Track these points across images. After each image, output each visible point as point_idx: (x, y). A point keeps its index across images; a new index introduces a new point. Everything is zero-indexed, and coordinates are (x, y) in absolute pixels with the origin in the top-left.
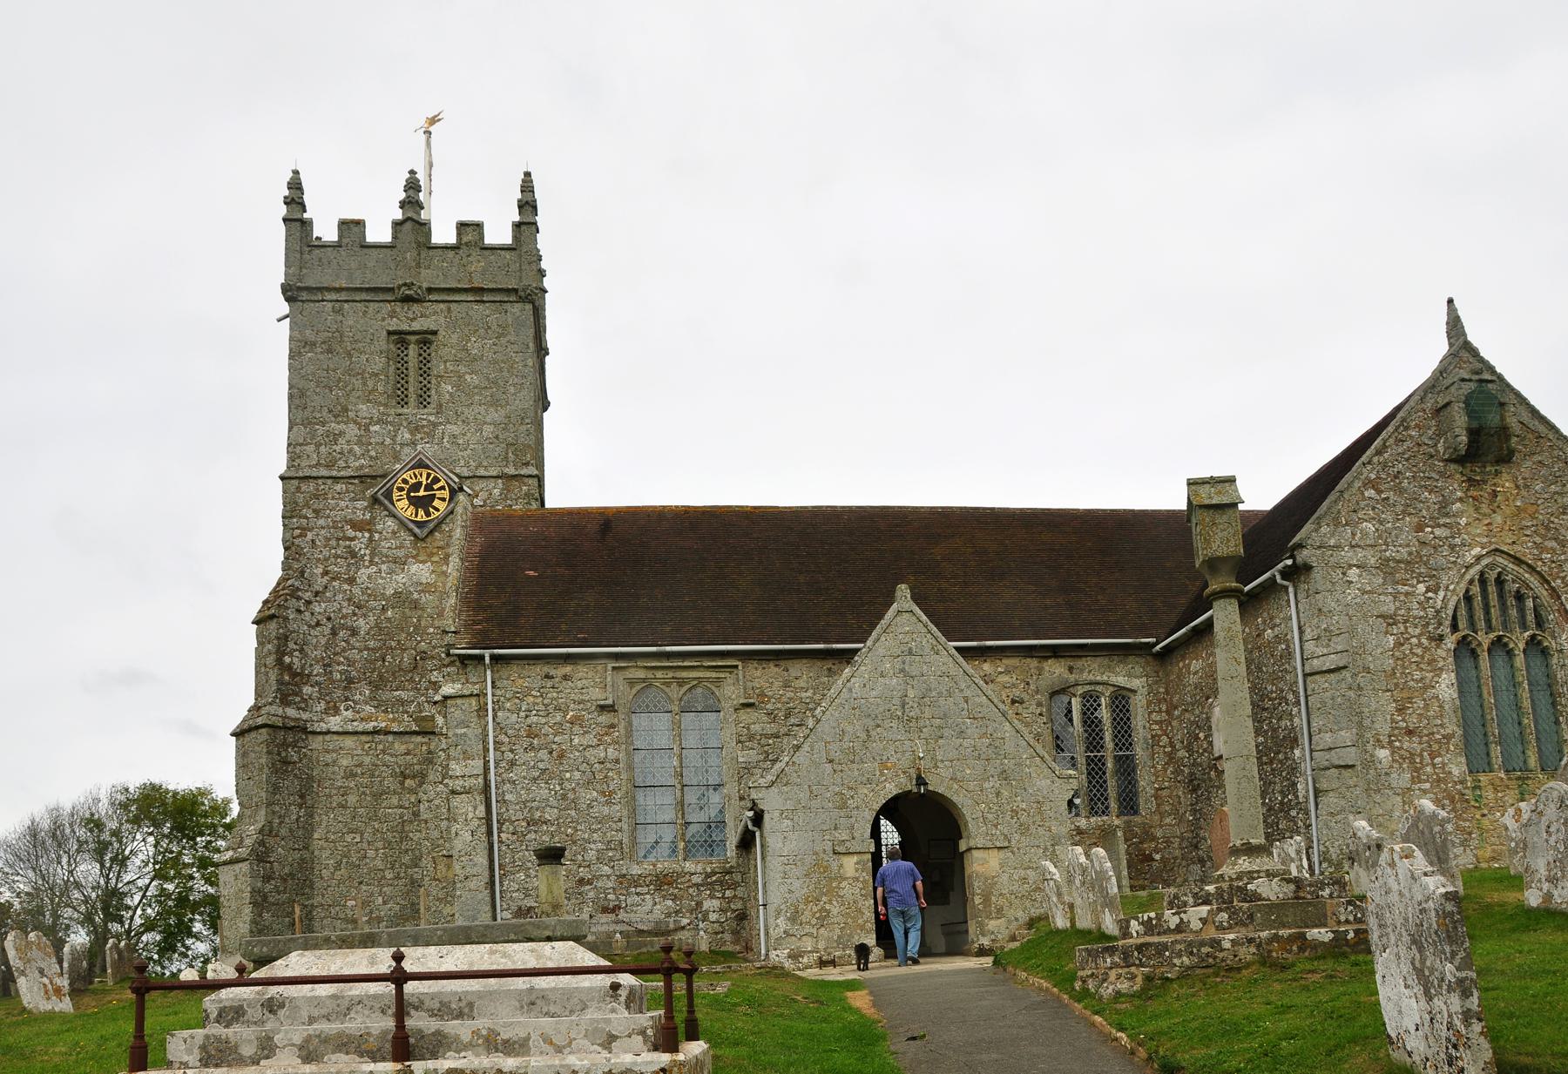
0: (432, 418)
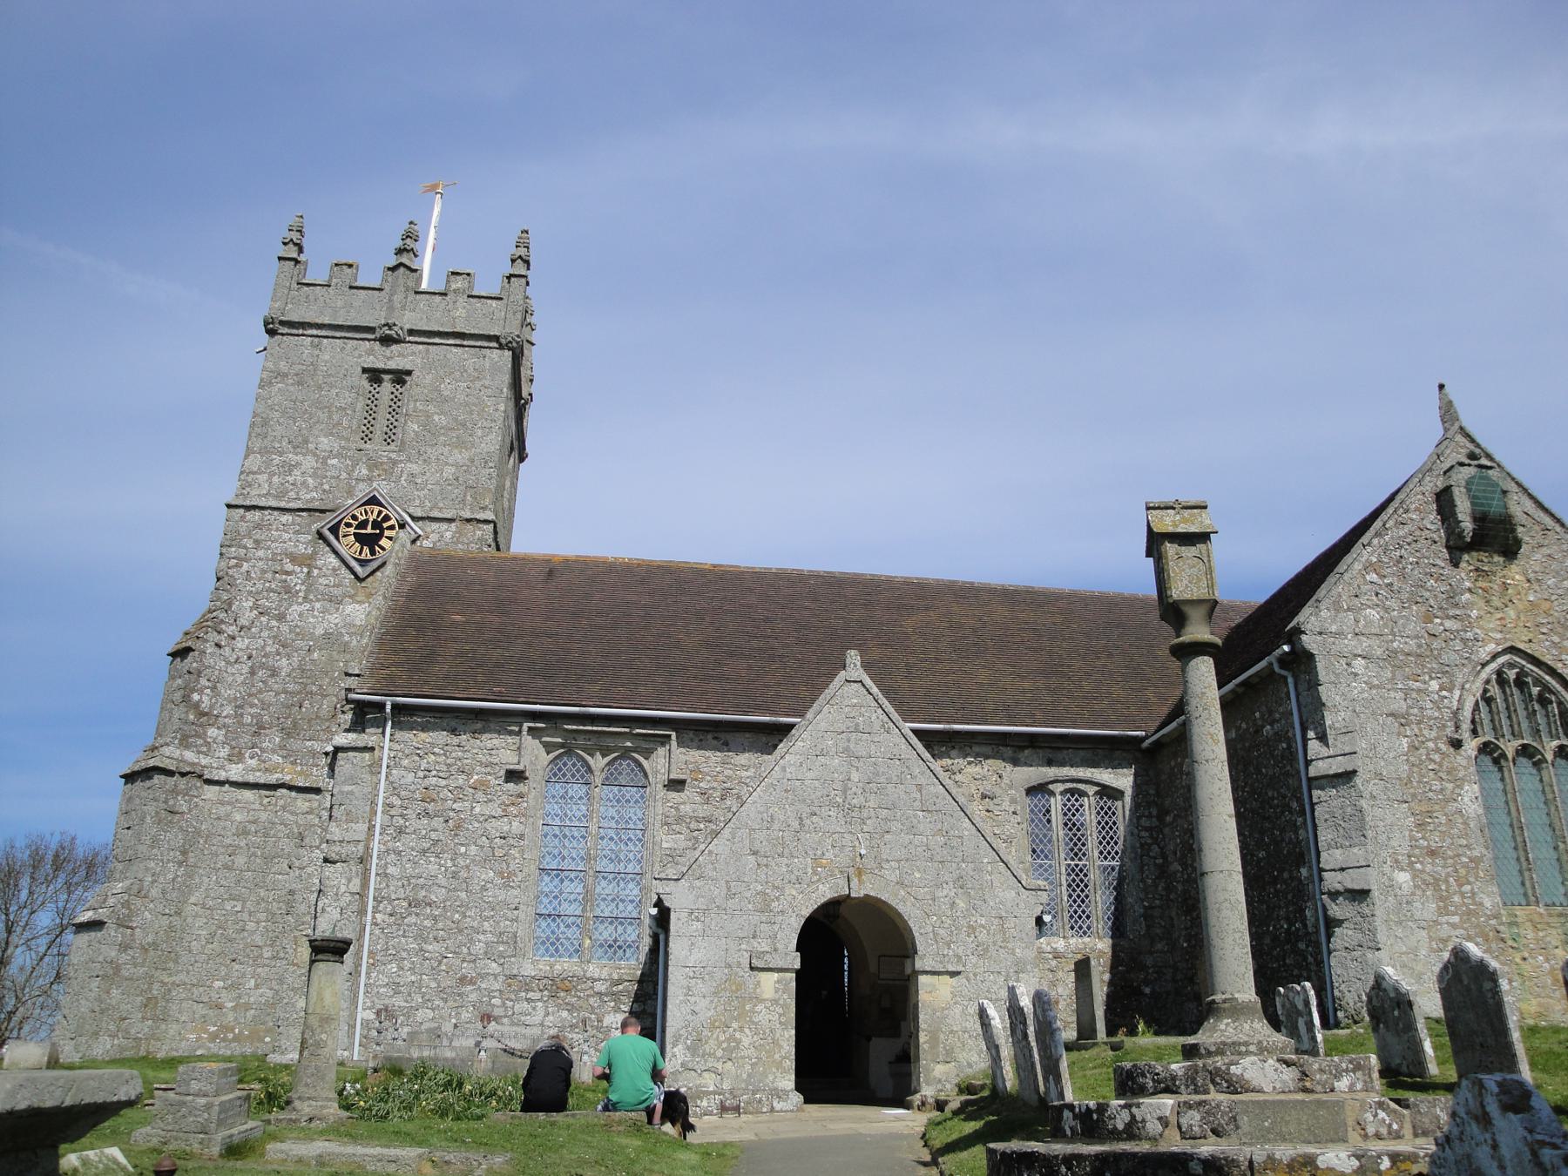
0: (393, 456)
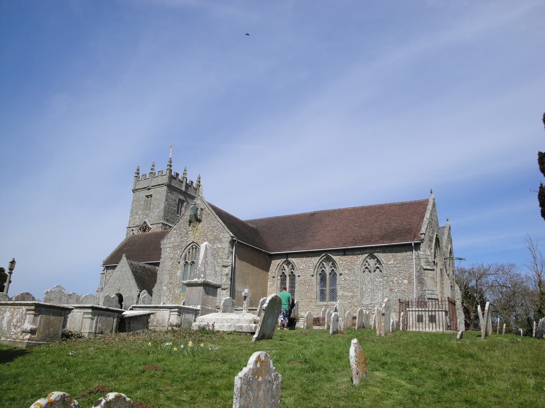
0: (149, 212)
